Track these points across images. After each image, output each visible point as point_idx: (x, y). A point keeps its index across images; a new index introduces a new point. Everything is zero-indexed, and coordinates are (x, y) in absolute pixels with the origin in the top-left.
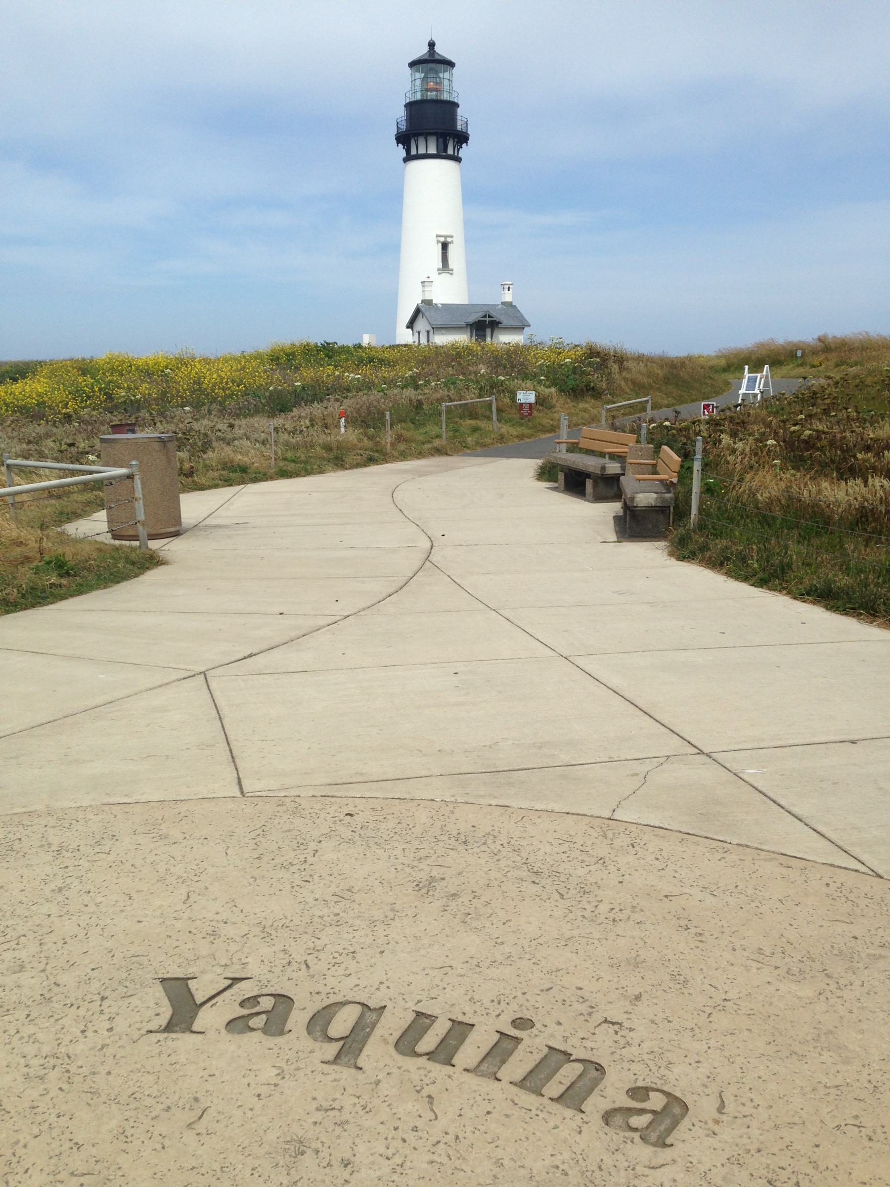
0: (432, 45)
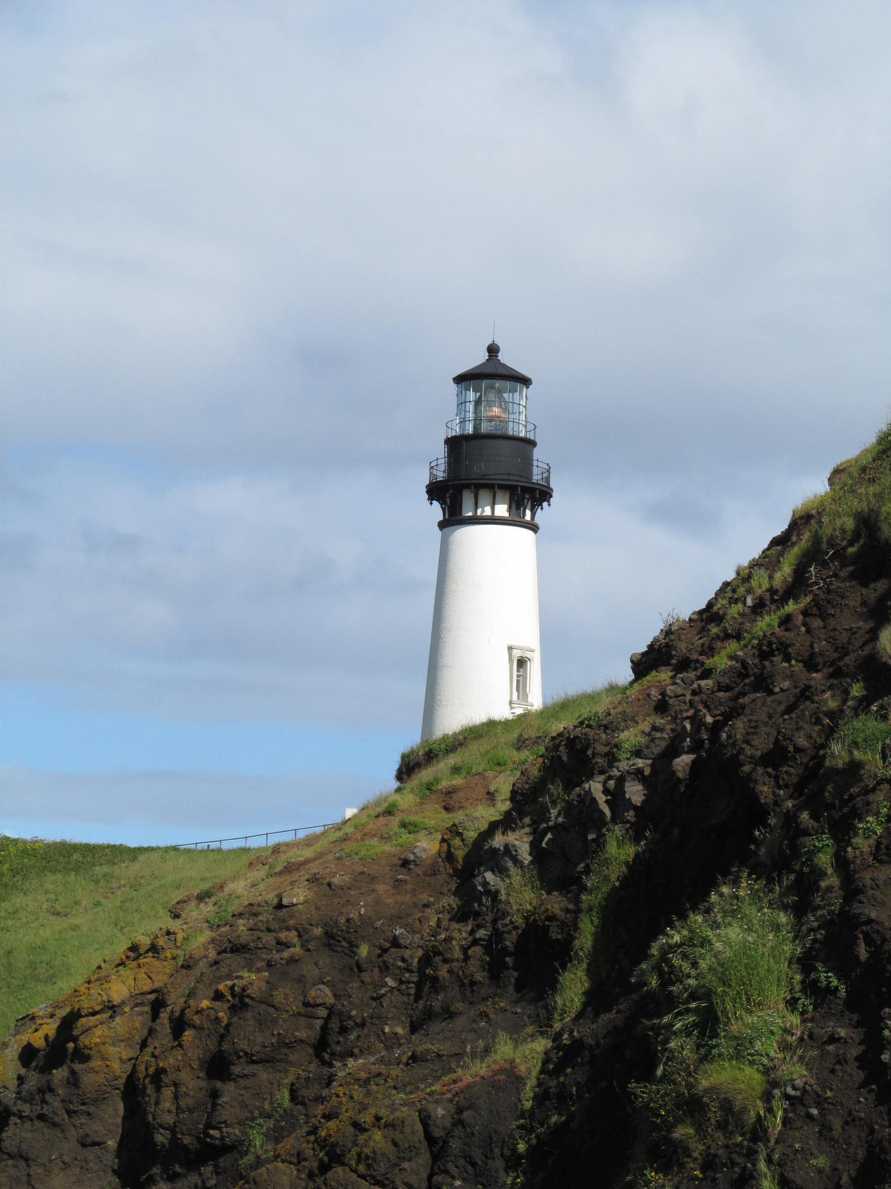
0: (493, 350)
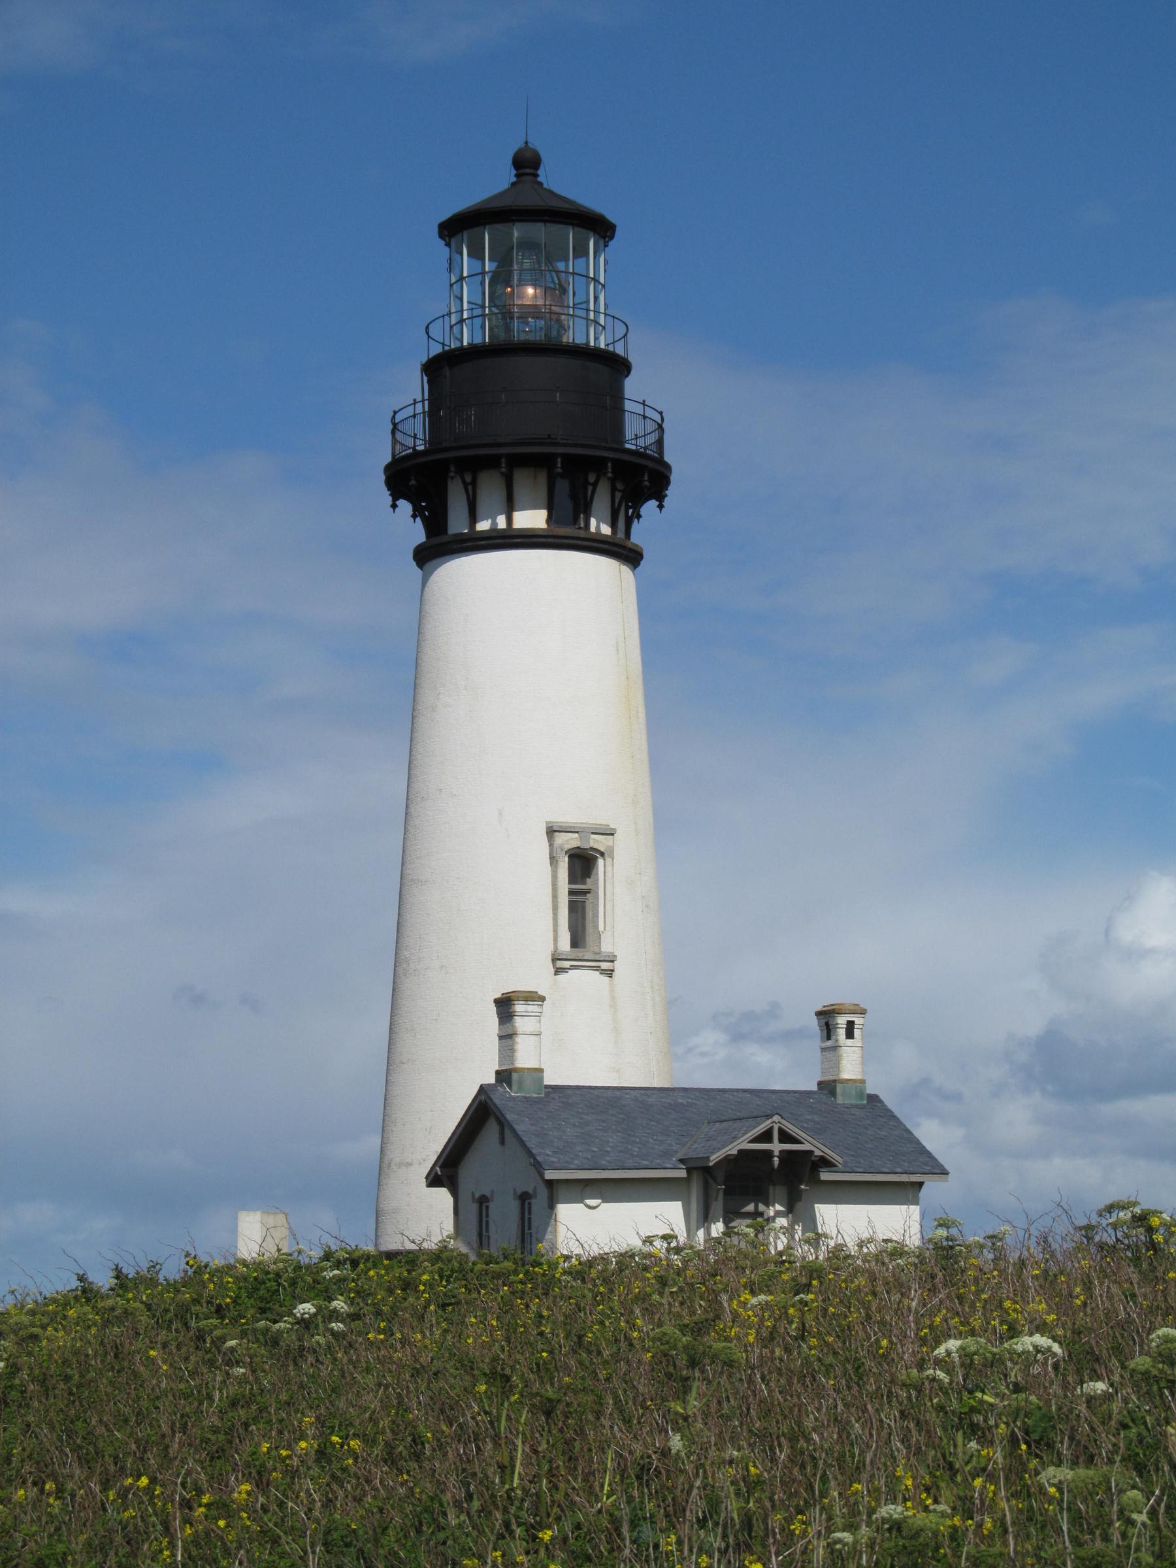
0: (526, 164)
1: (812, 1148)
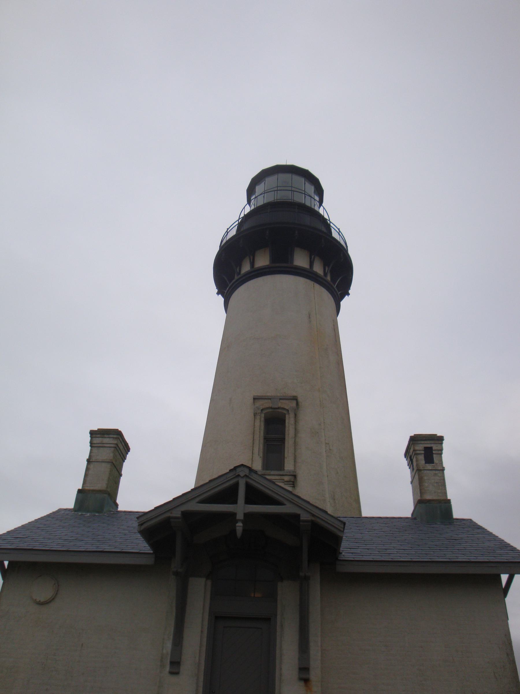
1: (297, 511)
